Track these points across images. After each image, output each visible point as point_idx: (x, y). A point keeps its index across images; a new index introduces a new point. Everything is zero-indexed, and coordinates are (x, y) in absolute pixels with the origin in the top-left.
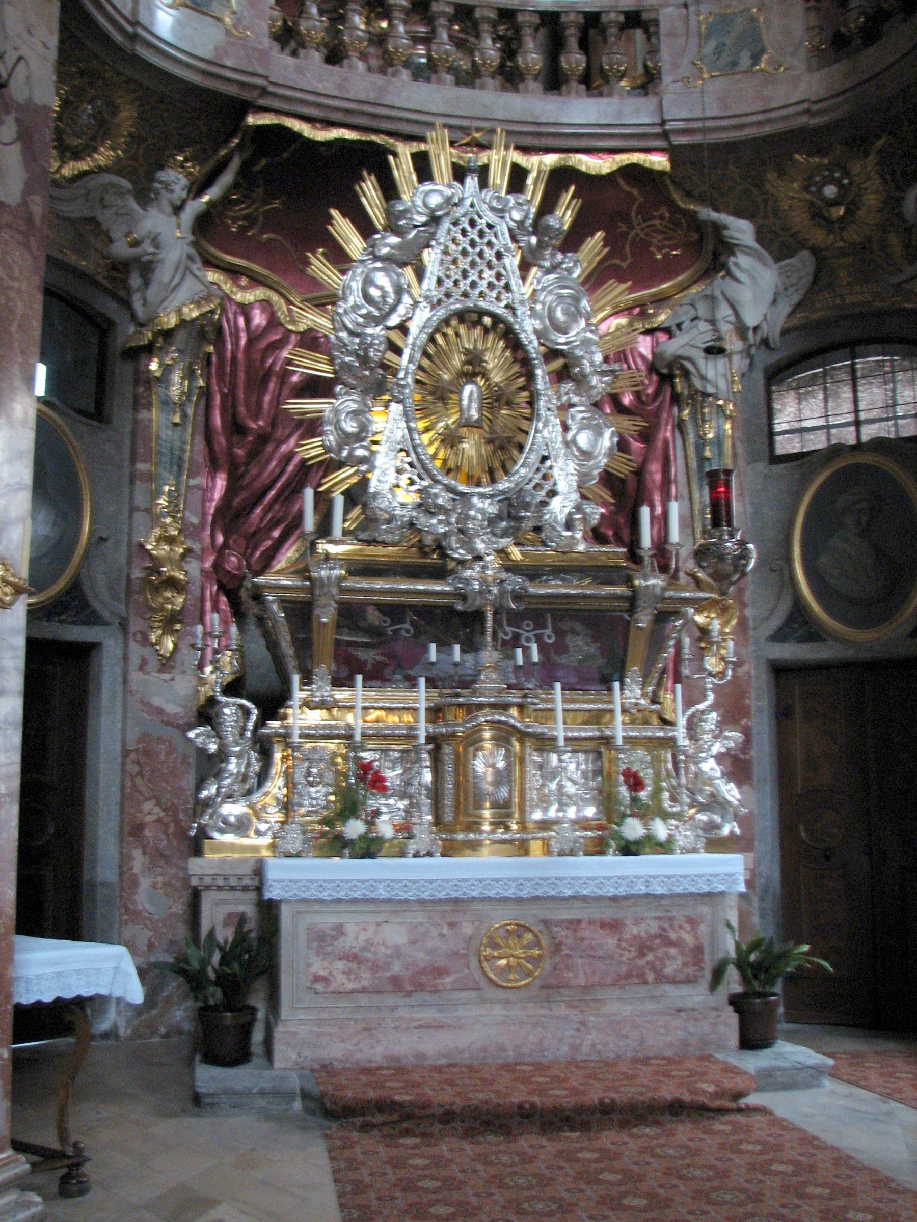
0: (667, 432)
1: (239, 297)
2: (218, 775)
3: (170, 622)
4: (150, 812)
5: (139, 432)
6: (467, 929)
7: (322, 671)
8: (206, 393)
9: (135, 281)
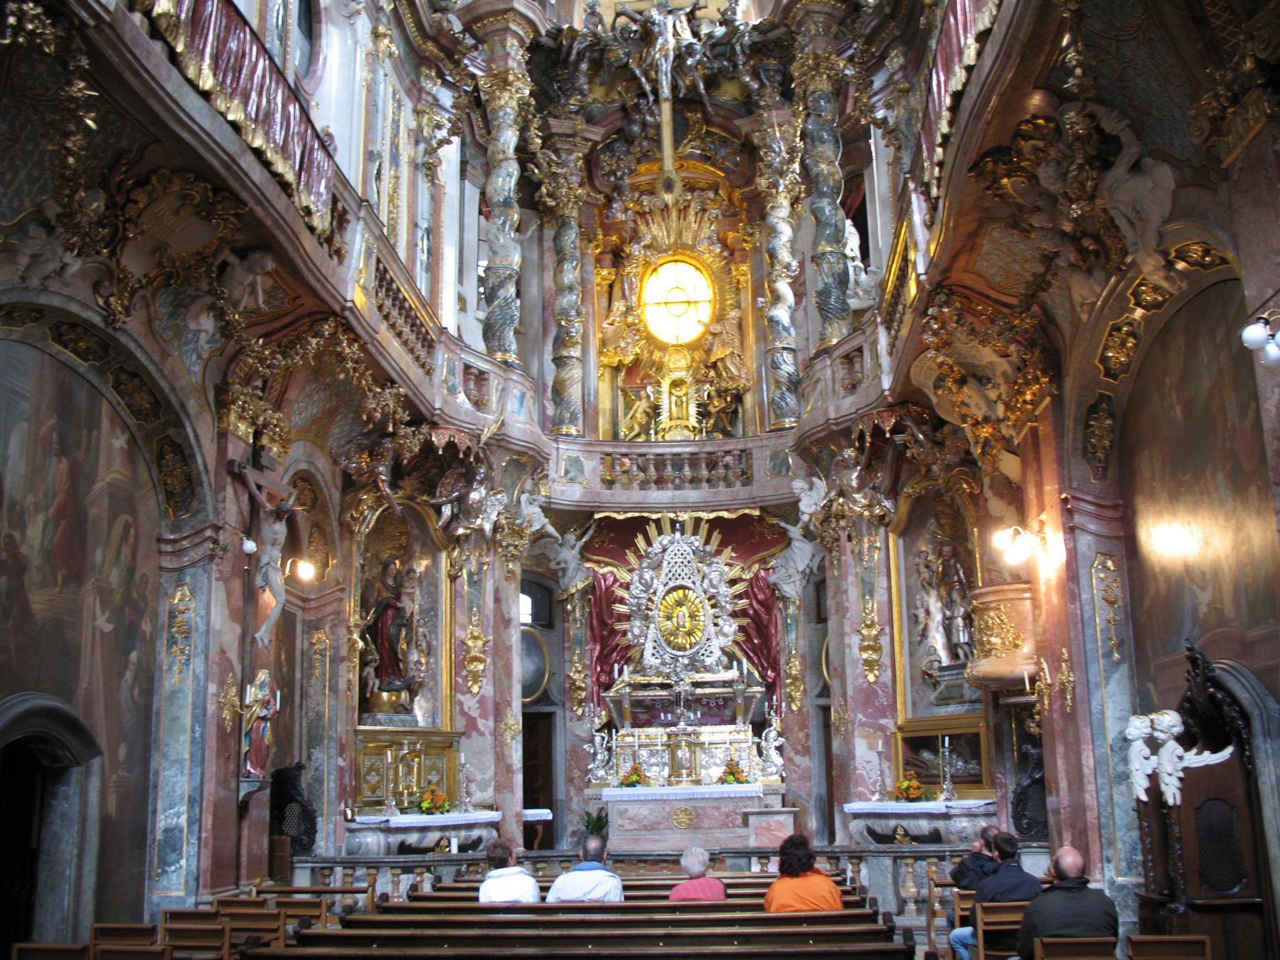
0: (775, 611)
2: (594, 760)
3: (580, 703)
4: (576, 773)
5: (565, 632)
6: (668, 809)
7: (627, 723)
8: (590, 613)
9: (560, 574)
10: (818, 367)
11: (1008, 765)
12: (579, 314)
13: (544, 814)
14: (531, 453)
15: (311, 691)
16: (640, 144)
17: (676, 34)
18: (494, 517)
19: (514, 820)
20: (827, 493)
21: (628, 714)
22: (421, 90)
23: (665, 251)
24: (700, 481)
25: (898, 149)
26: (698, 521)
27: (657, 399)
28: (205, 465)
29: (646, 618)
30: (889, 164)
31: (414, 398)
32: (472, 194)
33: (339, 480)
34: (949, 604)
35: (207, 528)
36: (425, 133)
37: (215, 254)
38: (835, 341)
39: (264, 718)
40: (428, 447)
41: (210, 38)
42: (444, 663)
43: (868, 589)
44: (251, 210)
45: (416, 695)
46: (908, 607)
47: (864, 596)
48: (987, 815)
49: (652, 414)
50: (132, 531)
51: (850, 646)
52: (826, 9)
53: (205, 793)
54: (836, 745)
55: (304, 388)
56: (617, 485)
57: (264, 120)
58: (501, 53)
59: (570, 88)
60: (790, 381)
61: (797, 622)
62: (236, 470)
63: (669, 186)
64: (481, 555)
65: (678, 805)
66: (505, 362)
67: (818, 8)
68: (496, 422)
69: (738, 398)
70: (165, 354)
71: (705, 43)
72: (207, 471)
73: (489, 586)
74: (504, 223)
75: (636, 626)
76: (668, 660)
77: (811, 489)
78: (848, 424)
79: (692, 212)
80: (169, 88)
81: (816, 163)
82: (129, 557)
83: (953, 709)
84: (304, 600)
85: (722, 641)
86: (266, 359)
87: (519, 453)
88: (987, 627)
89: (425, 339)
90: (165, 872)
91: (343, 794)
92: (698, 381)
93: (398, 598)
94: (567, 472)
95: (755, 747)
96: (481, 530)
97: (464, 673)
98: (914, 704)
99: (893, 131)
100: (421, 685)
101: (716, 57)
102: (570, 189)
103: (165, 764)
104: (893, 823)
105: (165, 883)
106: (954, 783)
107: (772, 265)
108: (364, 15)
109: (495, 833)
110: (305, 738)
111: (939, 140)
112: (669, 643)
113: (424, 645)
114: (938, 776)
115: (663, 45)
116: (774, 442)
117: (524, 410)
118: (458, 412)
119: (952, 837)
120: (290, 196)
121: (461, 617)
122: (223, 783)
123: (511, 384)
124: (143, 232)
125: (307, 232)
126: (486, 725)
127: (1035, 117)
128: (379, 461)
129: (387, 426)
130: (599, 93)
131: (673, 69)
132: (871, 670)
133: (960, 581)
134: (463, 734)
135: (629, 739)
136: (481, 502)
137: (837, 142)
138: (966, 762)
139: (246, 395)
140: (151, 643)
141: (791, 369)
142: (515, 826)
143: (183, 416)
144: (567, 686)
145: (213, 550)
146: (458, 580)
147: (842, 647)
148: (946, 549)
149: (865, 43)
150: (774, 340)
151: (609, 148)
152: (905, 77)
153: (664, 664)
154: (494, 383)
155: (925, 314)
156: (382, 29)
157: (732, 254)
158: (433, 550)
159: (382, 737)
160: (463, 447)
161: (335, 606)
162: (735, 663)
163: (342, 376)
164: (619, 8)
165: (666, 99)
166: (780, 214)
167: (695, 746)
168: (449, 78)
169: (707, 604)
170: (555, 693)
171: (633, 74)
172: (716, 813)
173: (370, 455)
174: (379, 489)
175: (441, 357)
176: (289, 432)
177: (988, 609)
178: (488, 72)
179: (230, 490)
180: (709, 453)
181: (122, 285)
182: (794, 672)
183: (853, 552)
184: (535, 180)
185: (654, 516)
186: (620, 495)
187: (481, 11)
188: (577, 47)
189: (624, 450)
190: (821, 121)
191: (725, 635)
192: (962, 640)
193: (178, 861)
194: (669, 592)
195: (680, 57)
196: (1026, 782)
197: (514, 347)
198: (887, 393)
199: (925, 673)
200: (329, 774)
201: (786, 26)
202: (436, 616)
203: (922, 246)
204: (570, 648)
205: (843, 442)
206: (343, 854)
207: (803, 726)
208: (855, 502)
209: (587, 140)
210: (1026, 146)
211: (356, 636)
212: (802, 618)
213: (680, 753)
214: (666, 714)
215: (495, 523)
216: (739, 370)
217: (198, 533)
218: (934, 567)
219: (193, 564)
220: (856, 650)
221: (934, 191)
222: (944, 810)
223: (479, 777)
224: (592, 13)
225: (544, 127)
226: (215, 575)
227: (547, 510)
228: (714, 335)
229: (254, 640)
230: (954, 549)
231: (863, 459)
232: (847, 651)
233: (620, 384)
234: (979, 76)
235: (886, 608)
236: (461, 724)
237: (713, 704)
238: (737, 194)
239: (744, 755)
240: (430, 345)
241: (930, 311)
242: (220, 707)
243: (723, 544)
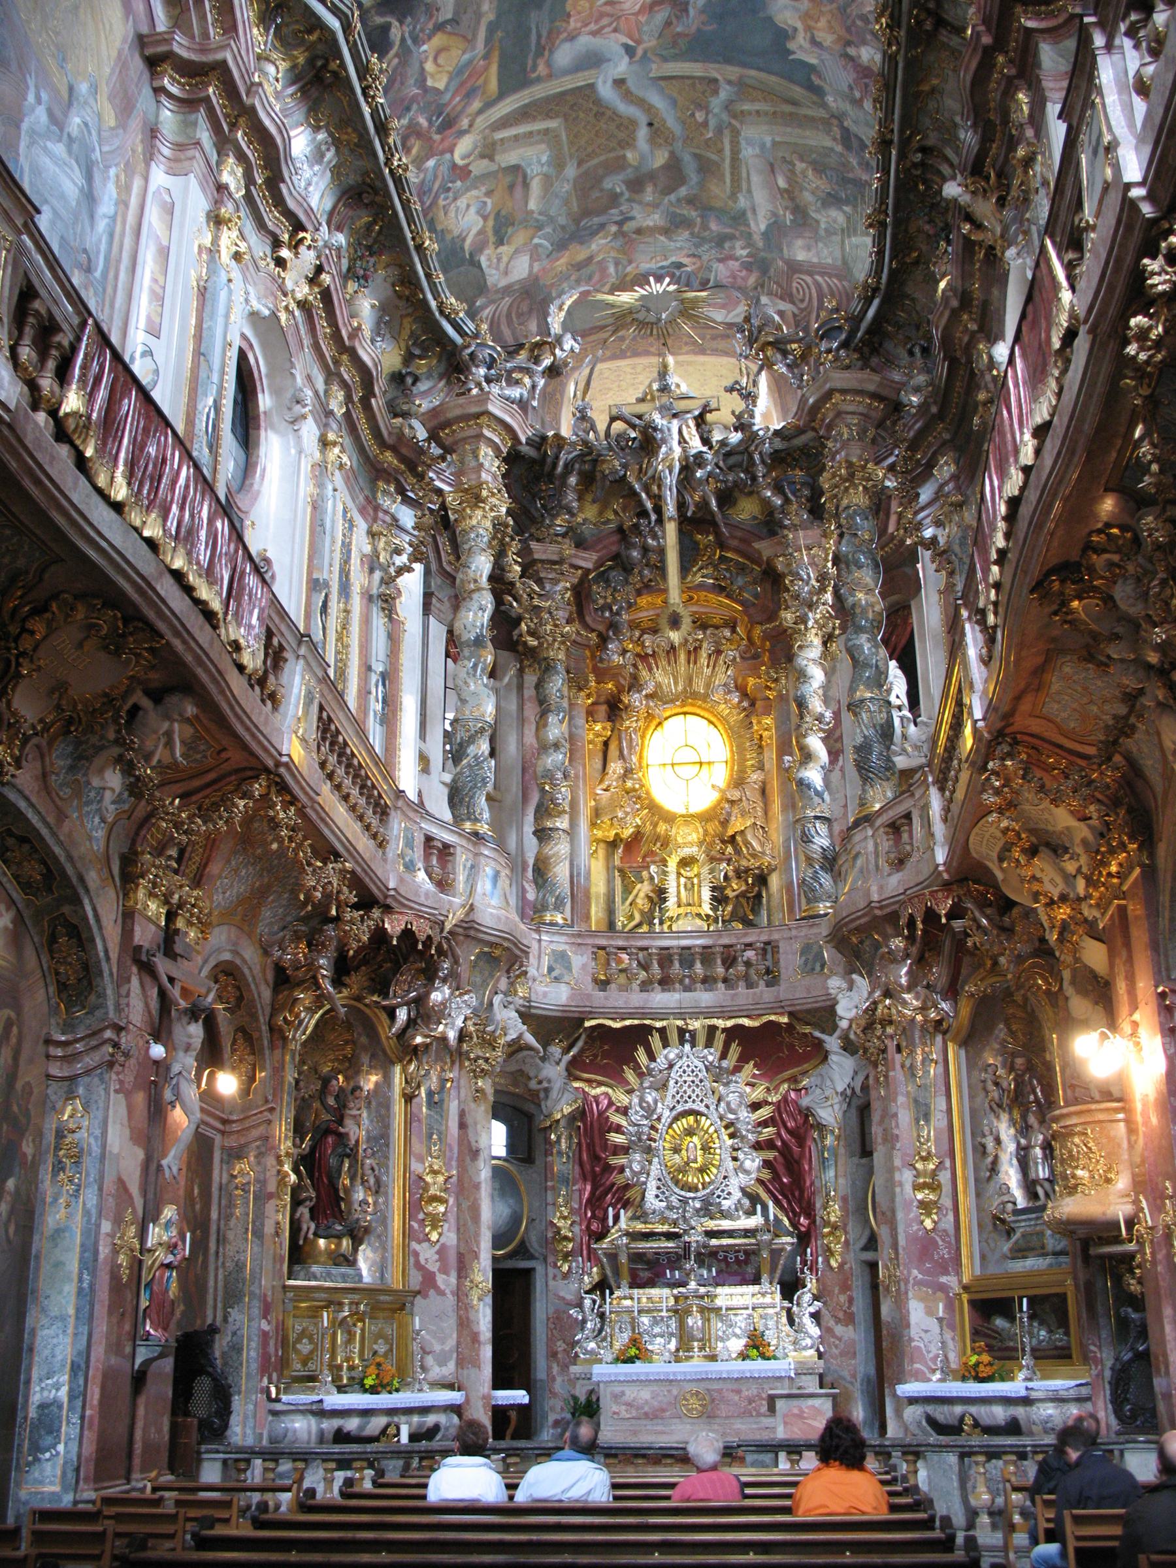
0: (809, 1142)
1: (594, 1092)
2: (583, 1329)
3: (566, 1256)
4: (560, 1346)
5: (547, 1168)
6: (675, 1392)
7: (624, 1283)
8: (579, 1144)
9: (542, 1095)
10: (857, 837)
11: (1104, 1334)
12: (566, 776)
13: (519, 1396)
14: (506, 944)
15: (230, 1235)
16: (640, 573)
17: (682, 441)
18: (459, 1023)
19: (480, 1403)
20: (871, 993)
21: (625, 1272)
22: (377, 508)
23: (672, 701)
24: (715, 980)
25: (951, 574)
26: (712, 1029)
27: (662, 881)
28: (106, 951)
29: (649, 1150)
30: (940, 592)
31: (363, 875)
32: (438, 632)
33: (270, 976)
34: (1024, 1130)
35: (106, 1028)
36: (382, 560)
37: (125, 696)
38: (877, 806)
39: (169, 1266)
40: (380, 935)
41: (125, 441)
42: (396, 1202)
43: (923, 1113)
44: (168, 643)
45: (361, 1244)
46: (973, 1134)
47: (917, 1121)
48: (1079, 1400)
49: (656, 899)
50: (15, 1030)
51: (901, 1184)
52: (861, 409)
53: (93, 1359)
54: (885, 1309)
55: (228, 861)
56: (613, 986)
57: (185, 537)
58: (473, 464)
59: (556, 506)
60: (825, 858)
61: (836, 1156)
62: (144, 958)
63: (675, 622)
64: (443, 1070)
65: (688, 1387)
66: (476, 834)
67: (851, 408)
68: (464, 906)
69: (762, 880)
70: (62, 816)
71: (717, 452)
72: (108, 959)
73: (453, 1107)
74: (475, 666)
75: (636, 1161)
76: (676, 1203)
77: (850, 989)
78: (896, 907)
79: (704, 654)
80: (75, 498)
81: (852, 591)
82: (10, 1061)
83: (1032, 1263)
84: (225, 1122)
85: (743, 1179)
86: (183, 823)
87: (491, 945)
88: (1071, 1156)
89: (377, 804)
90: (38, 1460)
91: (265, 1369)
92: (712, 859)
93: (340, 1121)
94: (551, 969)
95: (784, 1313)
96: (443, 1039)
97: (421, 1216)
98: (983, 1257)
99: (944, 552)
100: (367, 1230)
101: (730, 468)
102: (556, 626)
103: (44, 1321)
104: (958, 1409)
105: (37, 1474)
106: (1036, 1358)
107: (802, 717)
108: (310, 420)
109: (456, 1419)
110: (220, 1293)
111: (994, 556)
112: (677, 1182)
113: (372, 1181)
114: (1016, 1349)
115: (667, 454)
116: (805, 932)
117: (499, 891)
118: (417, 894)
119: (1034, 1428)
120: (215, 627)
121: (417, 1147)
122: (114, 1347)
123: (483, 860)
124: (39, 669)
125: (236, 671)
126: (447, 1281)
127: (1108, 525)
128: (319, 952)
129: (329, 909)
130: (590, 512)
131: (680, 482)
132: (929, 1214)
133: (1037, 1101)
134: (419, 1292)
135: (627, 1303)
136: (443, 1004)
137: (877, 566)
138: (1050, 1331)
139: (156, 867)
140: (32, 1169)
141: (826, 843)
142: (482, 1410)
143: (81, 891)
144: (550, 1235)
145: (112, 1055)
146: (415, 1101)
147: (891, 1185)
148: (1019, 1061)
149: (907, 449)
150: (804, 808)
151: (603, 577)
152: (958, 488)
153: (670, 1208)
154: (462, 859)
155: (984, 768)
156: (331, 436)
157: (753, 704)
158: (384, 1063)
159: (316, 1295)
160: (422, 937)
161: (261, 1130)
162: (759, 1207)
163: (275, 846)
164: (614, 411)
165: (670, 519)
166: (810, 654)
167: (709, 1311)
168: (410, 494)
169: (724, 1134)
170: (535, 1245)
171: (632, 488)
172: (736, 1398)
173: (309, 945)
174: (319, 987)
175: (397, 826)
176: (210, 914)
177: (1072, 1134)
178: (458, 487)
179: (135, 982)
180: (725, 946)
181: (13, 731)
182: (833, 1219)
183: (903, 1066)
184: (514, 615)
185: (658, 1024)
186: (615, 998)
187: (450, 415)
188: (563, 457)
189: (620, 943)
190: (857, 541)
191: (747, 1172)
192: (1041, 1175)
193: (54, 1446)
194: (676, 1119)
195: (688, 467)
196: (1127, 1356)
197: (486, 815)
198: (941, 868)
199: (996, 1218)
200: (249, 1340)
201: (814, 429)
202: (388, 1146)
203: (979, 685)
204: (553, 1188)
205: (890, 930)
206: (265, 1442)
207: (845, 1287)
208: (905, 1003)
209: (577, 567)
210: (1098, 561)
211: (287, 1168)
212: (842, 1150)
213: (690, 1321)
214: (672, 1270)
215: (462, 1029)
216: (762, 845)
217: (94, 1034)
218: (1005, 1085)
219: (88, 1072)
220: (908, 1188)
221: (991, 619)
222: (1023, 1393)
223: (437, 1347)
224: (583, 417)
225: (525, 552)
227: (526, 1016)
228: (732, 803)
229: (160, 1168)
230: (1029, 1061)
231: (914, 950)
232: (898, 1190)
233: (617, 862)
234: (1038, 478)
235: (946, 1136)
236: (415, 1280)
237: (731, 1258)
238: (758, 631)
239: (771, 1324)
240: (383, 812)
241: (991, 765)
242: (115, 1251)
243: (743, 1059)
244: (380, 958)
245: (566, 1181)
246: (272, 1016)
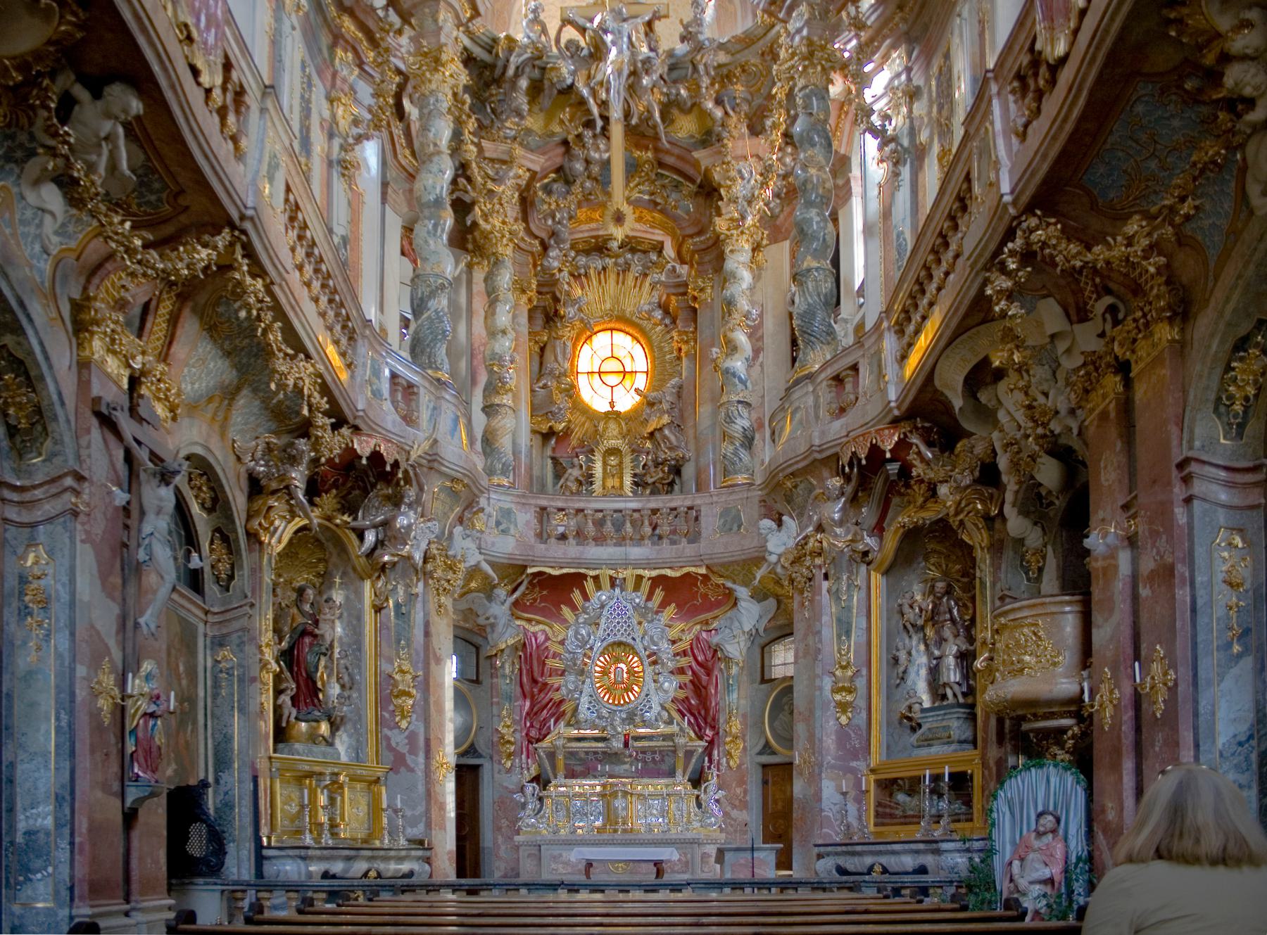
8: (520, 670)
29: (582, 672)
105: (29, 892)
133: (953, 620)
226: (80, 536)
244: (349, 485)
245: (510, 699)
246: (248, 520)
